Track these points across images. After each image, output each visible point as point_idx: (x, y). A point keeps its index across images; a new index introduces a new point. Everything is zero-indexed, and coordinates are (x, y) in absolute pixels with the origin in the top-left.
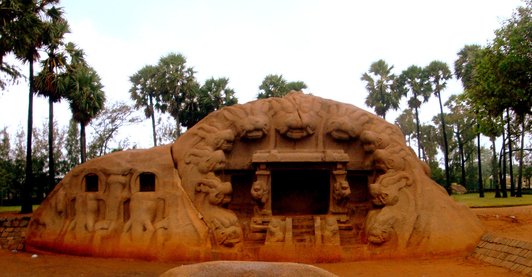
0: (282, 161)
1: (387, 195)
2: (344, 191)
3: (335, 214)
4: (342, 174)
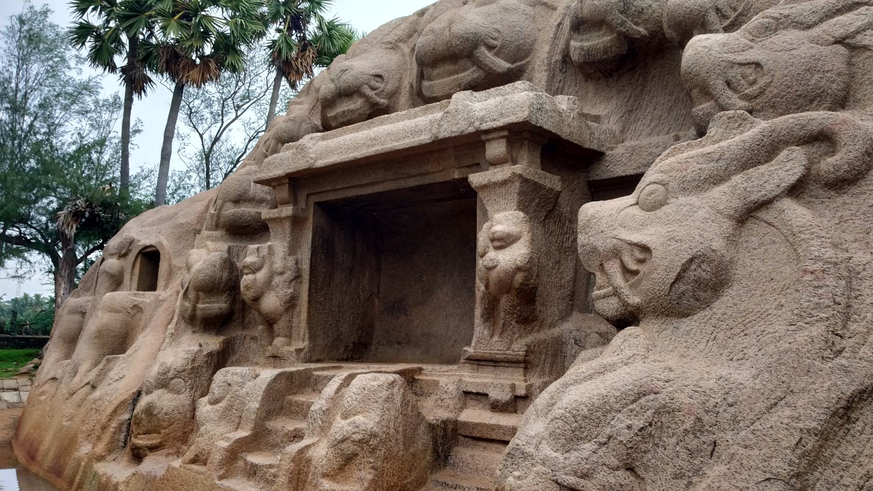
0: (320, 163)
1: (645, 249)
2: (492, 254)
3: (479, 362)
4: (504, 183)
